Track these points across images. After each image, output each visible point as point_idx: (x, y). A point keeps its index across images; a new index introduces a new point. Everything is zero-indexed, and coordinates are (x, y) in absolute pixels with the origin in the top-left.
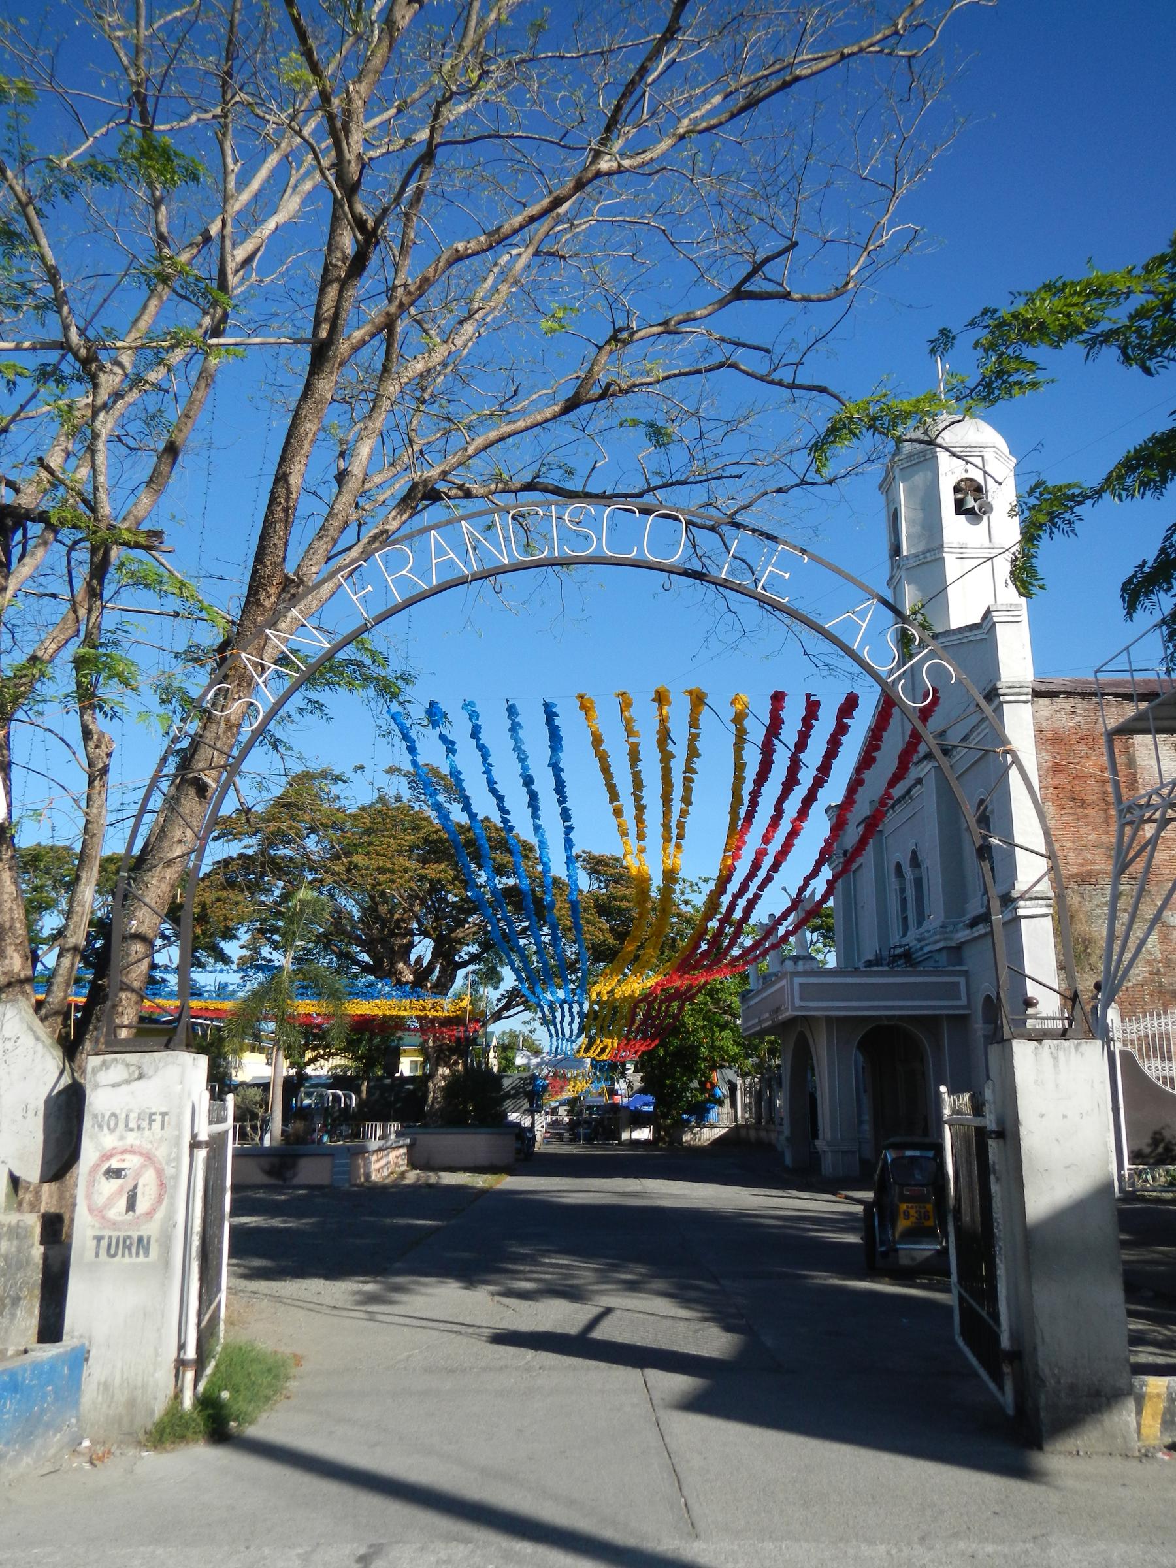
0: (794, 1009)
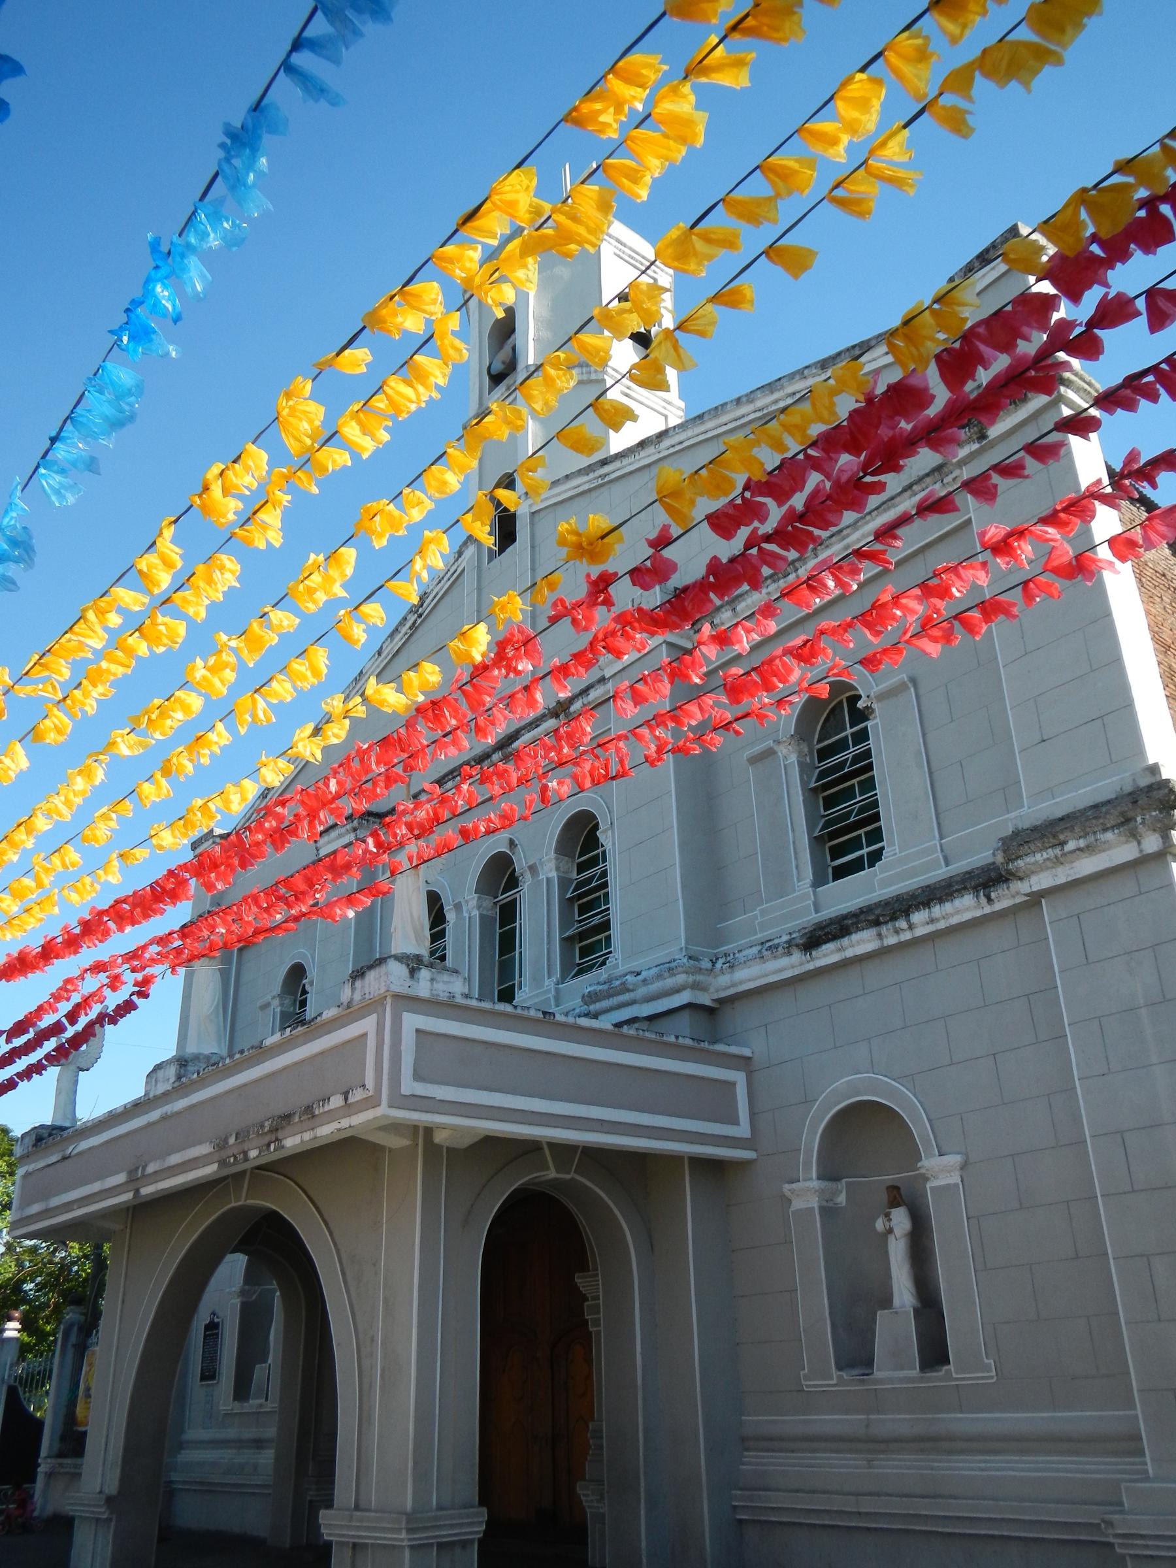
0: (400, 1100)
